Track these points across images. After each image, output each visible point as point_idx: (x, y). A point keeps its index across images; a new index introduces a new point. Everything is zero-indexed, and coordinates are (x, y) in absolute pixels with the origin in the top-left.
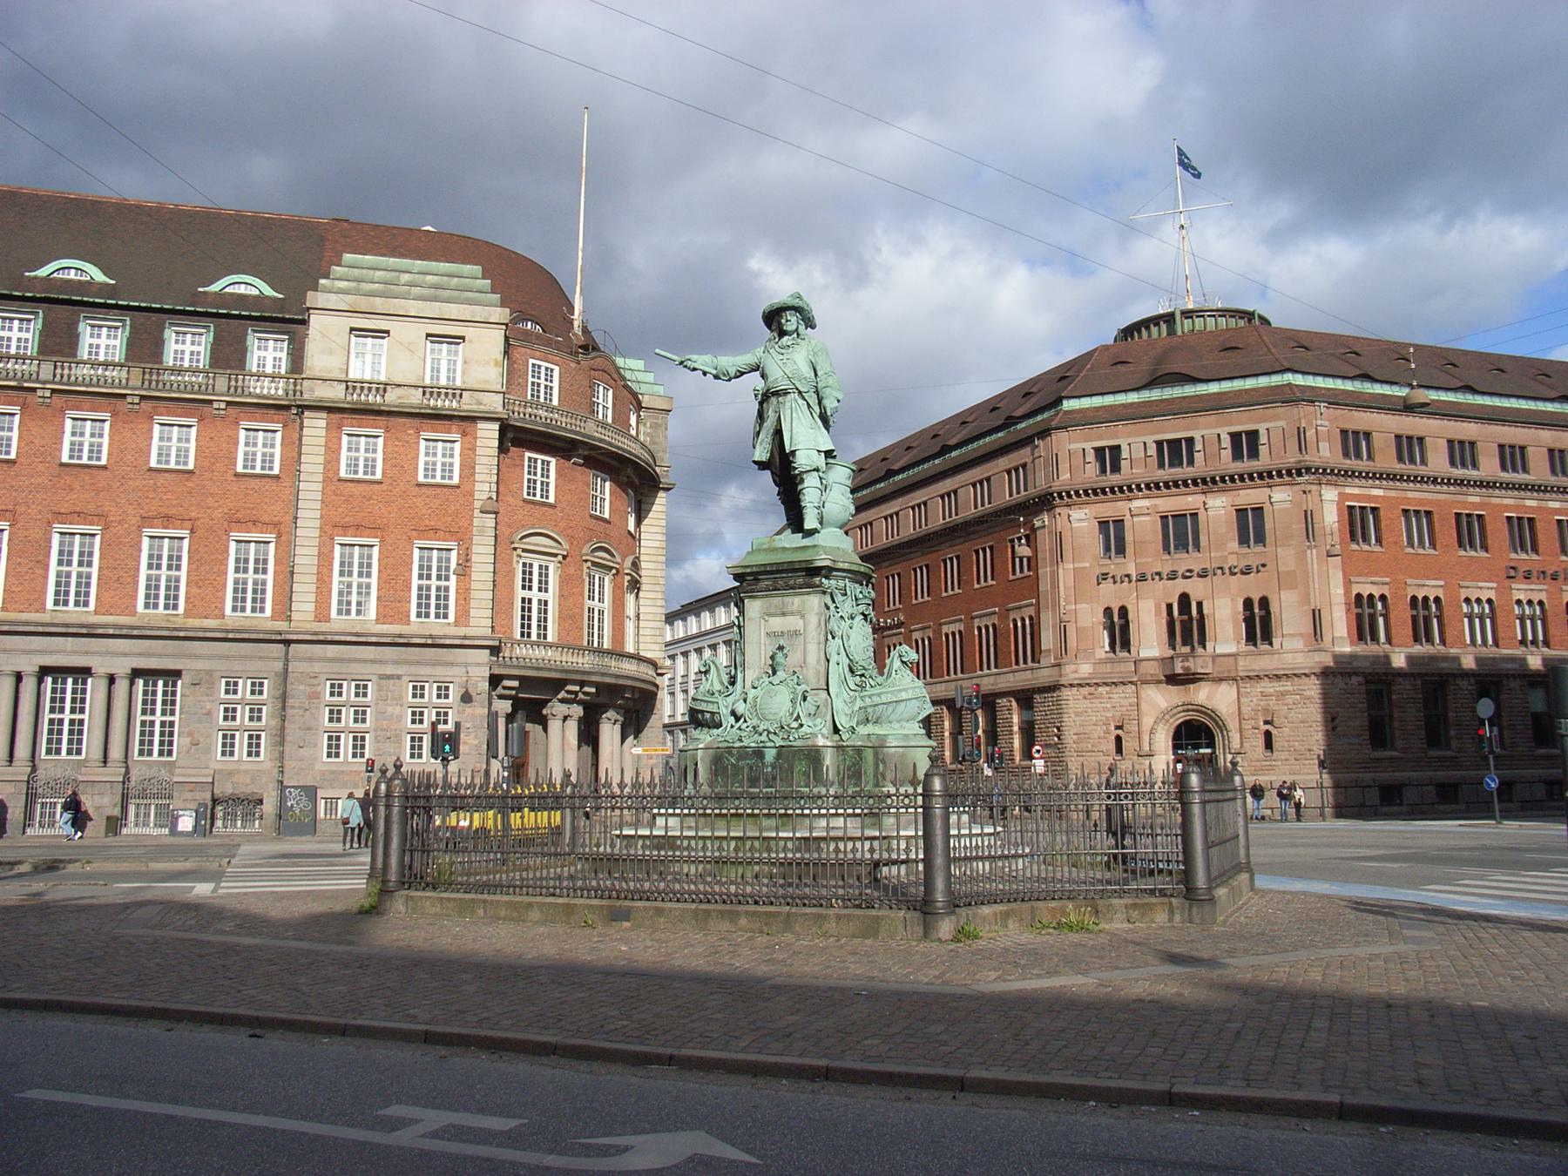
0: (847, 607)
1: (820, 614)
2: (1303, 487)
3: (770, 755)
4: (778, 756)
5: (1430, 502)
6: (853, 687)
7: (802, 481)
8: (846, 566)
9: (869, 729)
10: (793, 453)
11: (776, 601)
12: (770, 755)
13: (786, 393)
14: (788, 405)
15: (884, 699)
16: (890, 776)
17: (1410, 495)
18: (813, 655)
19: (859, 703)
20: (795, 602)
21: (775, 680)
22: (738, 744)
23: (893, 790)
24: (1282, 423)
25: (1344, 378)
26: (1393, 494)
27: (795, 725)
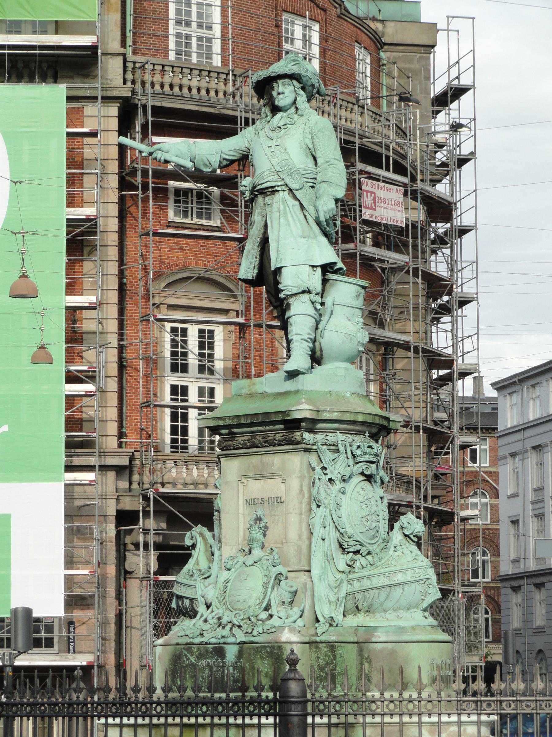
0: (340, 467)
1: (302, 478)
3: (231, 652)
6: (342, 566)
7: (288, 307)
8: (334, 416)
9: (360, 619)
10: (278, 270)
11: (255, 460)
12: (231, 652)
13: (273, 191)
14: (275, 206)
15: (375, 582)
16: (376, 677)
18: (294, 528)
19: (345, 588)
20: (276, 460)
21: (250, 560)
22: (198, 640)
23: (377, 695)
27: (264, 615)
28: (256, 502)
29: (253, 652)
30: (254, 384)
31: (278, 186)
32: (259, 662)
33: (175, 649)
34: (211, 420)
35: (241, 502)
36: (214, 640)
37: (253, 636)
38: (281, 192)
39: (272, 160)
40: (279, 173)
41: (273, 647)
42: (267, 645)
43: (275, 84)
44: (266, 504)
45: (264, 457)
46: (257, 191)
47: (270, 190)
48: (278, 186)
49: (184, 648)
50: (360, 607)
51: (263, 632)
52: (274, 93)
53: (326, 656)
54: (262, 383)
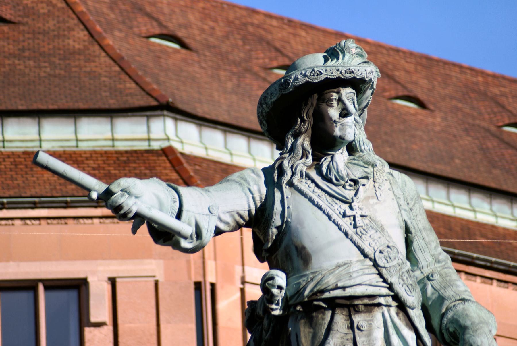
13: (371, 304)
31: (380, 296)
38: (385, 309)
40: (384, 271)
43: (335, 96)
46: (325, 300)
47: (366, 301)
48: (380, 296)
52: (334, 112)
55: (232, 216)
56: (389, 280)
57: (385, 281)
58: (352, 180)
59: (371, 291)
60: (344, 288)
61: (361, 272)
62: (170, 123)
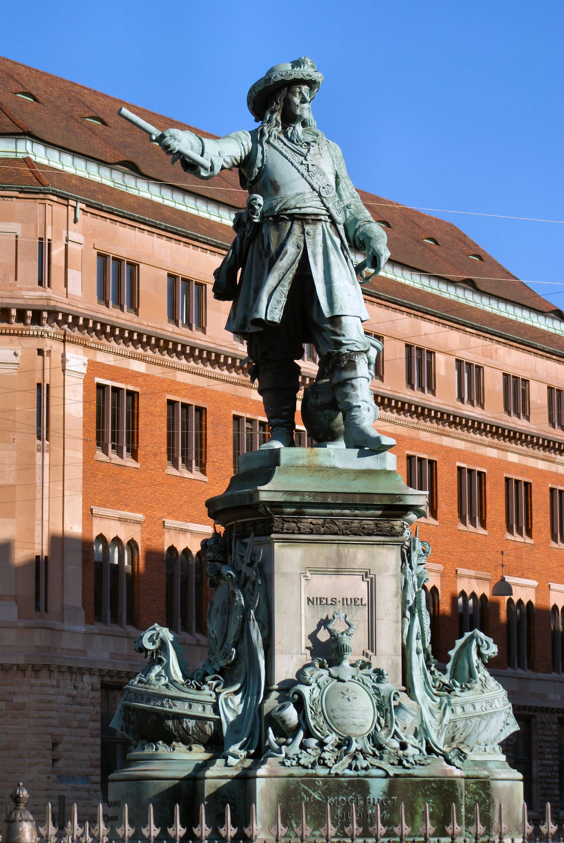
2: (35, 343)
3: (378, 788)
4: (391, 790)
5: (204, 392)
12: (378, 788)
13: (315, 219)
17: (181, 377)
20: (360, 554)
24: (16, 227)
25: (101, 162)
26: (157, 371)
28: (324, 601)
29: (410, 788)
30: (317, 455)
32: (420, 800)
33: (288, 782)
34: (281, 494)
35: (304, 601)
36: (348, 772)
37: (408, 768)
39: (311, 181)
40: (324, 200)
41: (442, 782)
42: (433, 779)
43: (298, 90)
44: (339, 605)
45: (342, 547)
46: (288, 215)
47: (313, 217)
49: (302, 781)
50: (456, 738)
51: (416, 764)
53: (475, 793)
54: (329, 455)
55: (231, 159)
56: (327, 205)
57: (325, 206)
58: (306, 143)
59: (316, 211)
60: (300, 208)
61: (311, 199)
62: (29, 144)
